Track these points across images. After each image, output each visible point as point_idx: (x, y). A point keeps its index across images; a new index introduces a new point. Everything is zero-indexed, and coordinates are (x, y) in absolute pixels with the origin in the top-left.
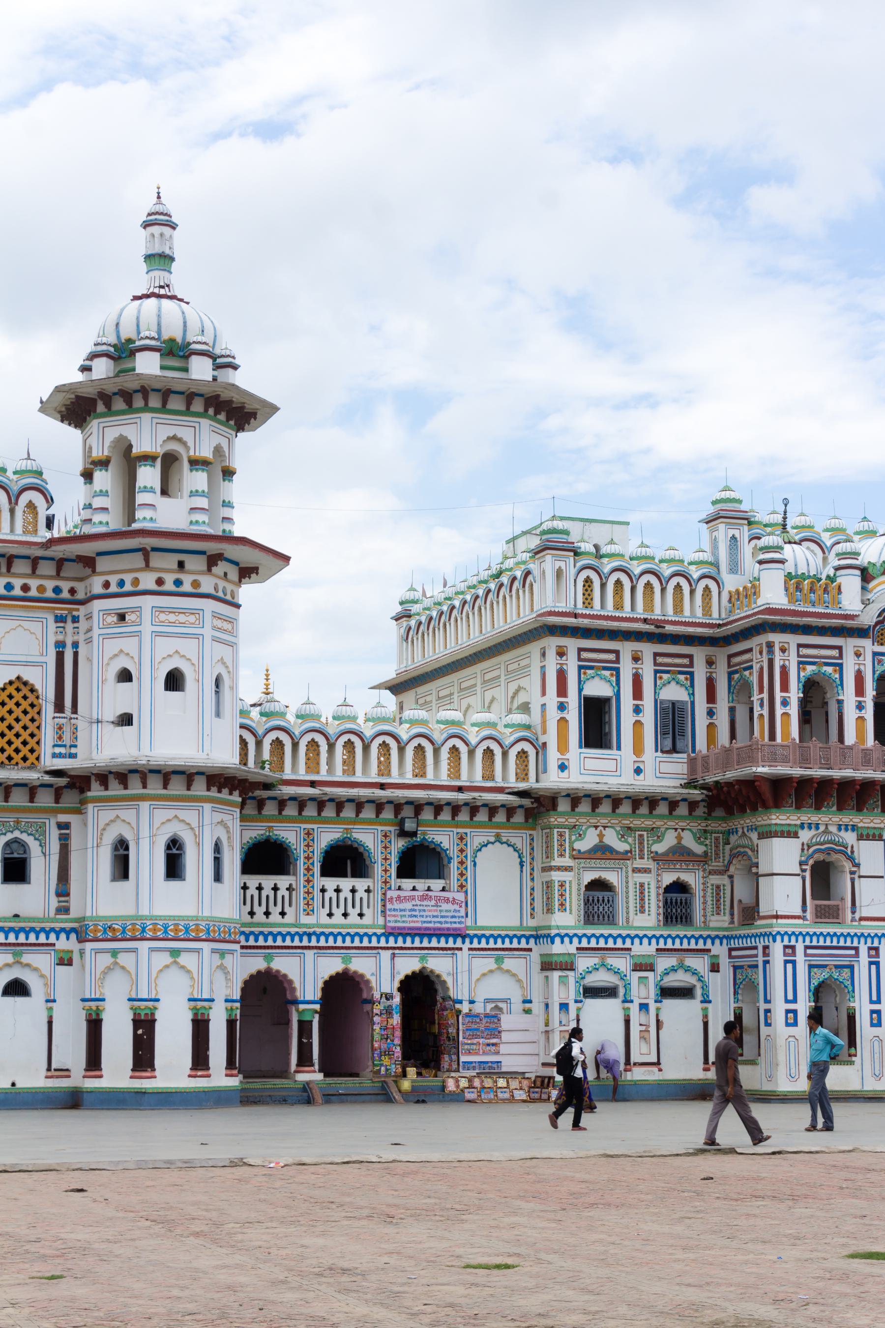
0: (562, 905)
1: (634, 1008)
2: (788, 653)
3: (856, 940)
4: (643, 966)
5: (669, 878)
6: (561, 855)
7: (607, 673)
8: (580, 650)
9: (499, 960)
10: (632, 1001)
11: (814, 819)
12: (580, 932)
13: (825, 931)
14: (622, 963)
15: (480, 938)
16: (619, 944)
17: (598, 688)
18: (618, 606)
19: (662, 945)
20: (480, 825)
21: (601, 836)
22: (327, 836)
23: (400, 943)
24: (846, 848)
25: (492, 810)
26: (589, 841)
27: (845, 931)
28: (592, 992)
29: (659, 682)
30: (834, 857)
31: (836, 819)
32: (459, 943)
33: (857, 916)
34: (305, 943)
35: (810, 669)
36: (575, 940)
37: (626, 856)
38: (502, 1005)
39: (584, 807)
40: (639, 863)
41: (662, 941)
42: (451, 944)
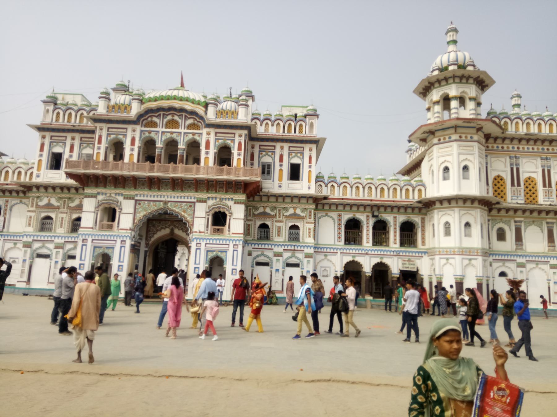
0: (29, 224)
1: (53, 262)
4: (59, 247)
5: (75, 216)
7: (61, 144)
8: (51, 136)
9: (15, 244)
10: (51, 260)
11: (104, 191)
12: (34, 234)
14: (51, 246)
15: (8, 236)
16: (49, 239)
18: (69, 121)
19: (67, 240)
20: (14, 197)
21: (49, 200)
24: (118, 202)
25: (17, 192)
26: (45, 201)
27: (111, 234)
28: (39, 256)
29: (82, 147)
36: (32, 237)
37: (58, 208)
38: (16, 260)
39: (42, 190)
40: (62, 210)
41: (67, 238)
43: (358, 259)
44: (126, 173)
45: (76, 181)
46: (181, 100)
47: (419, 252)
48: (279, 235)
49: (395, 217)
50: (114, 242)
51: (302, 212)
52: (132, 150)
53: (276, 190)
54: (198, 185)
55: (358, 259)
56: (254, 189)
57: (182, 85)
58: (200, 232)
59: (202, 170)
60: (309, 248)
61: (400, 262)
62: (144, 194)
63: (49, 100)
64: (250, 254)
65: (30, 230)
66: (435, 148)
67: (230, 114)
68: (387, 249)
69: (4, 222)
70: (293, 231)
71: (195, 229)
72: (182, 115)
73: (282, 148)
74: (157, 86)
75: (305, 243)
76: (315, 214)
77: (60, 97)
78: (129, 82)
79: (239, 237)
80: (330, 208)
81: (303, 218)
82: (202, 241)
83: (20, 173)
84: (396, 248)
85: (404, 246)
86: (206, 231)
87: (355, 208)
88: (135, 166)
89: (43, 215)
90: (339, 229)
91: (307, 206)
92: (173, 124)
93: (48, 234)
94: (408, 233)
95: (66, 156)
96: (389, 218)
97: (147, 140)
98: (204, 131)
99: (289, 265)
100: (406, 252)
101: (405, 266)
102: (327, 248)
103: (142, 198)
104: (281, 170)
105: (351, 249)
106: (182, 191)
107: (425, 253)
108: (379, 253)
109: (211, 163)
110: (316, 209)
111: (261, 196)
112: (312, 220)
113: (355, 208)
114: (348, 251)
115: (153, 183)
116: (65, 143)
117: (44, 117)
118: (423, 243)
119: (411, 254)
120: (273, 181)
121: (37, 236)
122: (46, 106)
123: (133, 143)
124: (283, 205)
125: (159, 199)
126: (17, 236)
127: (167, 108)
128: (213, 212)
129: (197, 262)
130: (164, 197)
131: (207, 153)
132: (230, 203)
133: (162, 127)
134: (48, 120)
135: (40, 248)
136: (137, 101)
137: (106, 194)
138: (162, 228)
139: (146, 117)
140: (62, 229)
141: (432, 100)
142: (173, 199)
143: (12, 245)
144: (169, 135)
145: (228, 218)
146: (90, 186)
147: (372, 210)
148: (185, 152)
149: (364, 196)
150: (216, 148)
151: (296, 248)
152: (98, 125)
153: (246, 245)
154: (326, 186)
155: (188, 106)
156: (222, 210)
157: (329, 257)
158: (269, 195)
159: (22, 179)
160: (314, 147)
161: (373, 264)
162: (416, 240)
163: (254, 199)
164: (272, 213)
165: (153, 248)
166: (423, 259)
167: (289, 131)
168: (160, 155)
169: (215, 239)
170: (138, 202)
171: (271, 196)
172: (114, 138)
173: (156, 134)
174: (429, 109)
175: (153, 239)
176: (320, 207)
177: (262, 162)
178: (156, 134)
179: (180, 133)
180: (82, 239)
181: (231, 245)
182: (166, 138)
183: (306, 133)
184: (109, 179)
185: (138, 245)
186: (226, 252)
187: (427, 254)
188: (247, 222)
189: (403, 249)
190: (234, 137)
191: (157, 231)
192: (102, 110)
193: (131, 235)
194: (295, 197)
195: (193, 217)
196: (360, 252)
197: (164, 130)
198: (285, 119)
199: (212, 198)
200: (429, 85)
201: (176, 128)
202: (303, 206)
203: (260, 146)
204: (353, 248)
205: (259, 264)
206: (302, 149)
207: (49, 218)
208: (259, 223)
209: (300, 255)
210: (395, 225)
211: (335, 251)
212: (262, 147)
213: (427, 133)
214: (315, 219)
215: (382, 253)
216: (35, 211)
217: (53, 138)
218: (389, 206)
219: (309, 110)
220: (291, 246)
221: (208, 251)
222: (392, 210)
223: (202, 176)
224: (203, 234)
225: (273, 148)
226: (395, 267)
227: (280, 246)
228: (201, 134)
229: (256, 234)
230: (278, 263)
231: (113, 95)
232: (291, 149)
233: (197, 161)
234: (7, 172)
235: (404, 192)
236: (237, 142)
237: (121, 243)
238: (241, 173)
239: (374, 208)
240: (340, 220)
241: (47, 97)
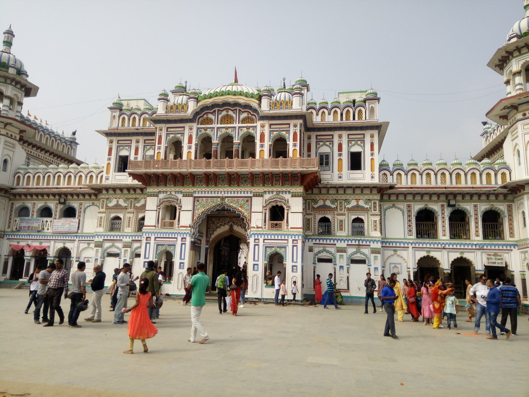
0: (100, 225)
1: (122, 260)
2: (162, 131)
3: (176, 235)
5: (141, 216)
6: (103, 208)
7: (127, 147)
9: (89, 244)
11: (164, 189)
12: (104, 234)
13: (163, 231)
14: (120, 245)
15: (82, 236)
16: (118, 238)
17: (124, 153)
18: (133, 125)
19: (134, 239)
20: (87, 200)
21: (118, 201)
22: (40, 204)
23: (57, 238)
24: (178, 200)
25: (90, 195)
26: (114, 203)
28: (110, 255)
30: (173, 204)
31: (173, 189)
32: (75, 238)
33: (180, 225)
34: (28, 238)
35: (171, 135)
36: (103, 237)
37: (126, 208)
38: (90, 259)
39: (111, 192)
40: (129, 210)
41: (134, 237)
42: (73, 239)
43: (433, 254)
44: (184, 170)
45: (139, 182)
46: (235, 95)
47: (506, 245)
48: (341, 229)
49: (475, 206)
50: (175, 239)
51: (366, 203)
52: (190, 148)
53: (336, 181)
54: (254, 179)
55: (432, 254)
56: (311, 180)
57: (236, 81)
58: (258, 227)
59: (257, 163)
60: (375, 243)
61: (485, 257)
62: (201, 191)
63: (115, 106)
64: (311, 250)
65: (101, 230)
66: (519, 125)
67: (284, 105)
68: (468, 242)
69: (79, 224)
70: (356, 224)
71: (253, 224)
72: (236, 109)
73: (340, 136)
74: (211, 83)
75: (370, 237)
76: (380, 206)
77: (125, 103)
78: (186, 82)
79: (299, 232)
80: (397, 198)
81: (367, 210)
82: (260, 236)
83: (91, 177)
84: (479, 241)
85: (488, 239)
86: (263, 227)
87: (426, 198)
88: (193, 163)
89: (113, 215)
90: (410, 221)
91: (371, 197)
92: (228, 119)
93: (117, 234)
94: (492, 224)
95: (132, 158)
96: (468, 207)
97: (203, 137)
98: (259, 124)
99: (354, 261)
100: (491, 245)
101: (490, 261)
102: (396, 243)
103: (200, 195)
104: (340, 160)
105: (424, 243)
106: (238, 185)
107: (514, 246)
108: (459, 247)
109: (266, 156)
110: (382, 200)
111: (320, 188)
112: (377, 212)
113: (426, 198)
114: (421, 246)
115: (210, 179)
116: (130, 147)
117: (111, 123)
118: (512, 234)
119: (497, 248)
120: (332, 172)
121: (107, 236)
122: (112, 112)
123: (190, 141)
124: (344, 197)
125: (216, 195)
126: (90, 237)
127: (221, 103)
128: (270, 206)
129: (256, 259)
130: (221, 193)
131: (262, 146)
132: (287, 196)
133: (217, 124)
134: (115, 126)
135: (110, 247)
136: (193, 99)
137: (166, 192)
138: (221, 225)
139: (201, 115)
140: (130, 228)
141: (511, 71)
142: (229, 195)
143: (86, 245)
144: (224, 130)
145: (286, 211)
146: (152, 185)
147: (447, 198)
148: (240, 147)
149: (437, 183)
150: (271, 140)
151: (361, 243)
152: (158, 126)
153: (307, 240)
154: (392, 175)
155: (242, 100)
156: (279, 204)
157: (399, 253)
158: (329, 186)
159: (94, 182)
160: (376, 133)
161: (452, 259)
162: (503, 231)
163: (312, 192)
164: (333, 206)
165: (214, 245)
166: (512, 253)
167: (347, 118)
168: (217, 151)
169: (273, 234)
170: (196, 199)
171: (331, 187)
172: (173, 137)
173: (212, 131)
174: (508, 82)
175: (213, 236)
176: (386, 197)
177: (319, 153)
178: (212, 131)
179: (235, 127)
180: (145, 237)
181: (290, 241)
182: (221, 133)
183: (366, 119)
184: (169, 177)
185: (199, 242)
186: (285, 247)
187: (516, 247)
188: (306, 216)
189: (487, 242)
190: (289, 127)
191: (217, 227)
192: (161, 111)
193: (191, 231)
194: (356, 187)
195: (251, 212)
196: (436, 246)
197: (219, 125)
198: (342, 106)
199: (269, 193)
200: (507, 55)
201: (231, 123)
202: (366, 197)
203: (317, 136)
204: (427, 242)
205: (321, 260)
206: (362, 136)
207: (118, 218)
208: (319, 217)
209: (366, 251)
210: (476, 215)
211: (406, 245)
212: (319, 137)
213: (508, 108)
214: (380, 211)
215: (462, 247)
216: (105, 213)
217: (120, 142)
218: (468, 194)
219: (369, 94)
220: (355, 240)
221: (266, 247)
222: (471, 198)
223: (257, 169)
224: (261, 229)
225: (331, 137)
226: (479, 262)
227: (343, 241)
228: (256, 127)
229: (317, 229)
230: (341, 259)
231: (171, 97)
232: (350, 137)
233: (253, 155)
234: (81, 176)
235: (484, 176)
236: (292, 132)
237: (182, 241)
238: (297, 164)
239: (449, 196)
240: (409, 211)
241: (113, 104)
